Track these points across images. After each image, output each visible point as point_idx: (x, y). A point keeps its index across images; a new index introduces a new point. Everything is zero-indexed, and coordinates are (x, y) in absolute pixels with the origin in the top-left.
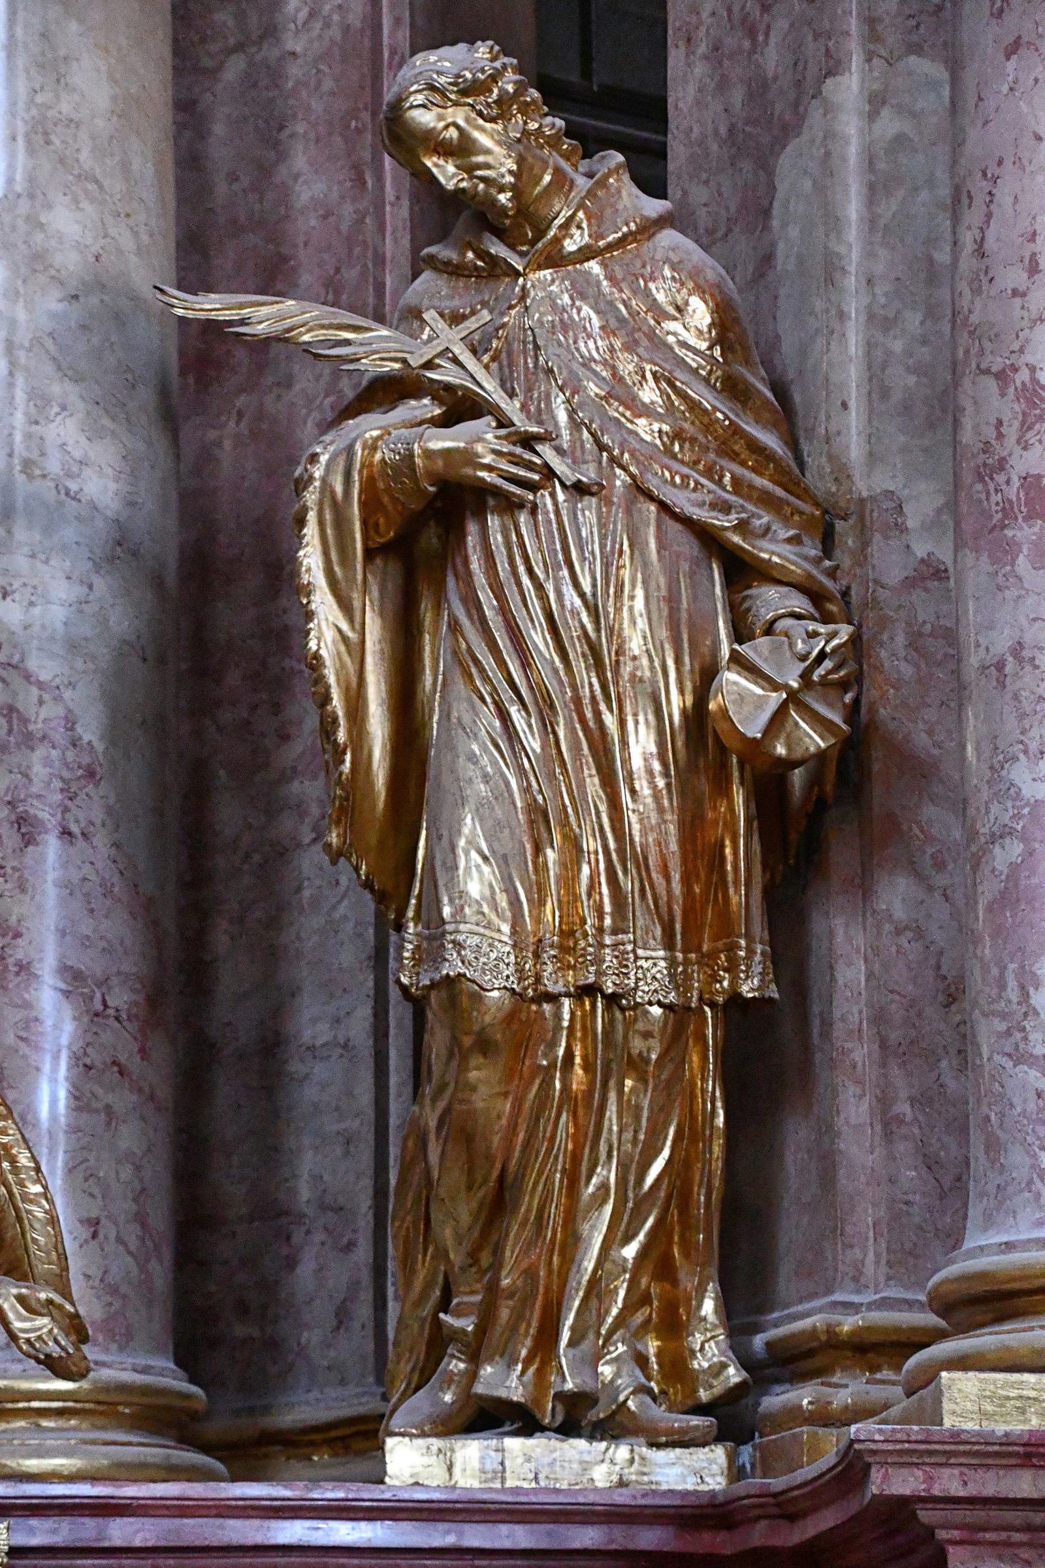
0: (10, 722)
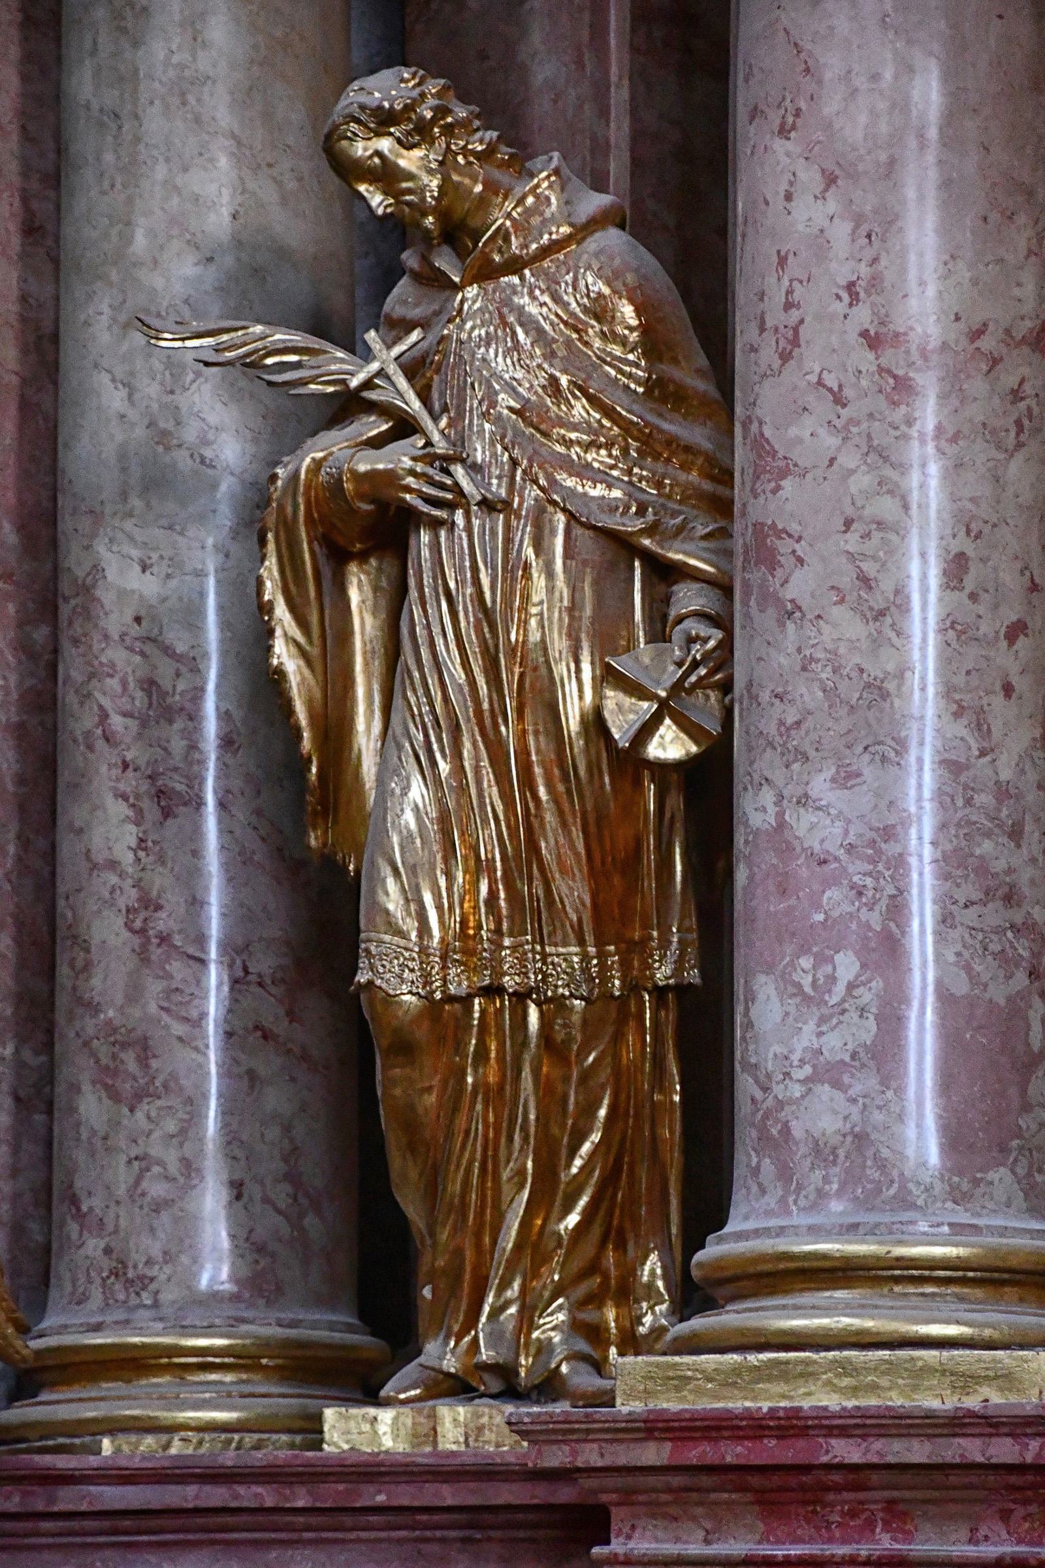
0: (150, 697)
